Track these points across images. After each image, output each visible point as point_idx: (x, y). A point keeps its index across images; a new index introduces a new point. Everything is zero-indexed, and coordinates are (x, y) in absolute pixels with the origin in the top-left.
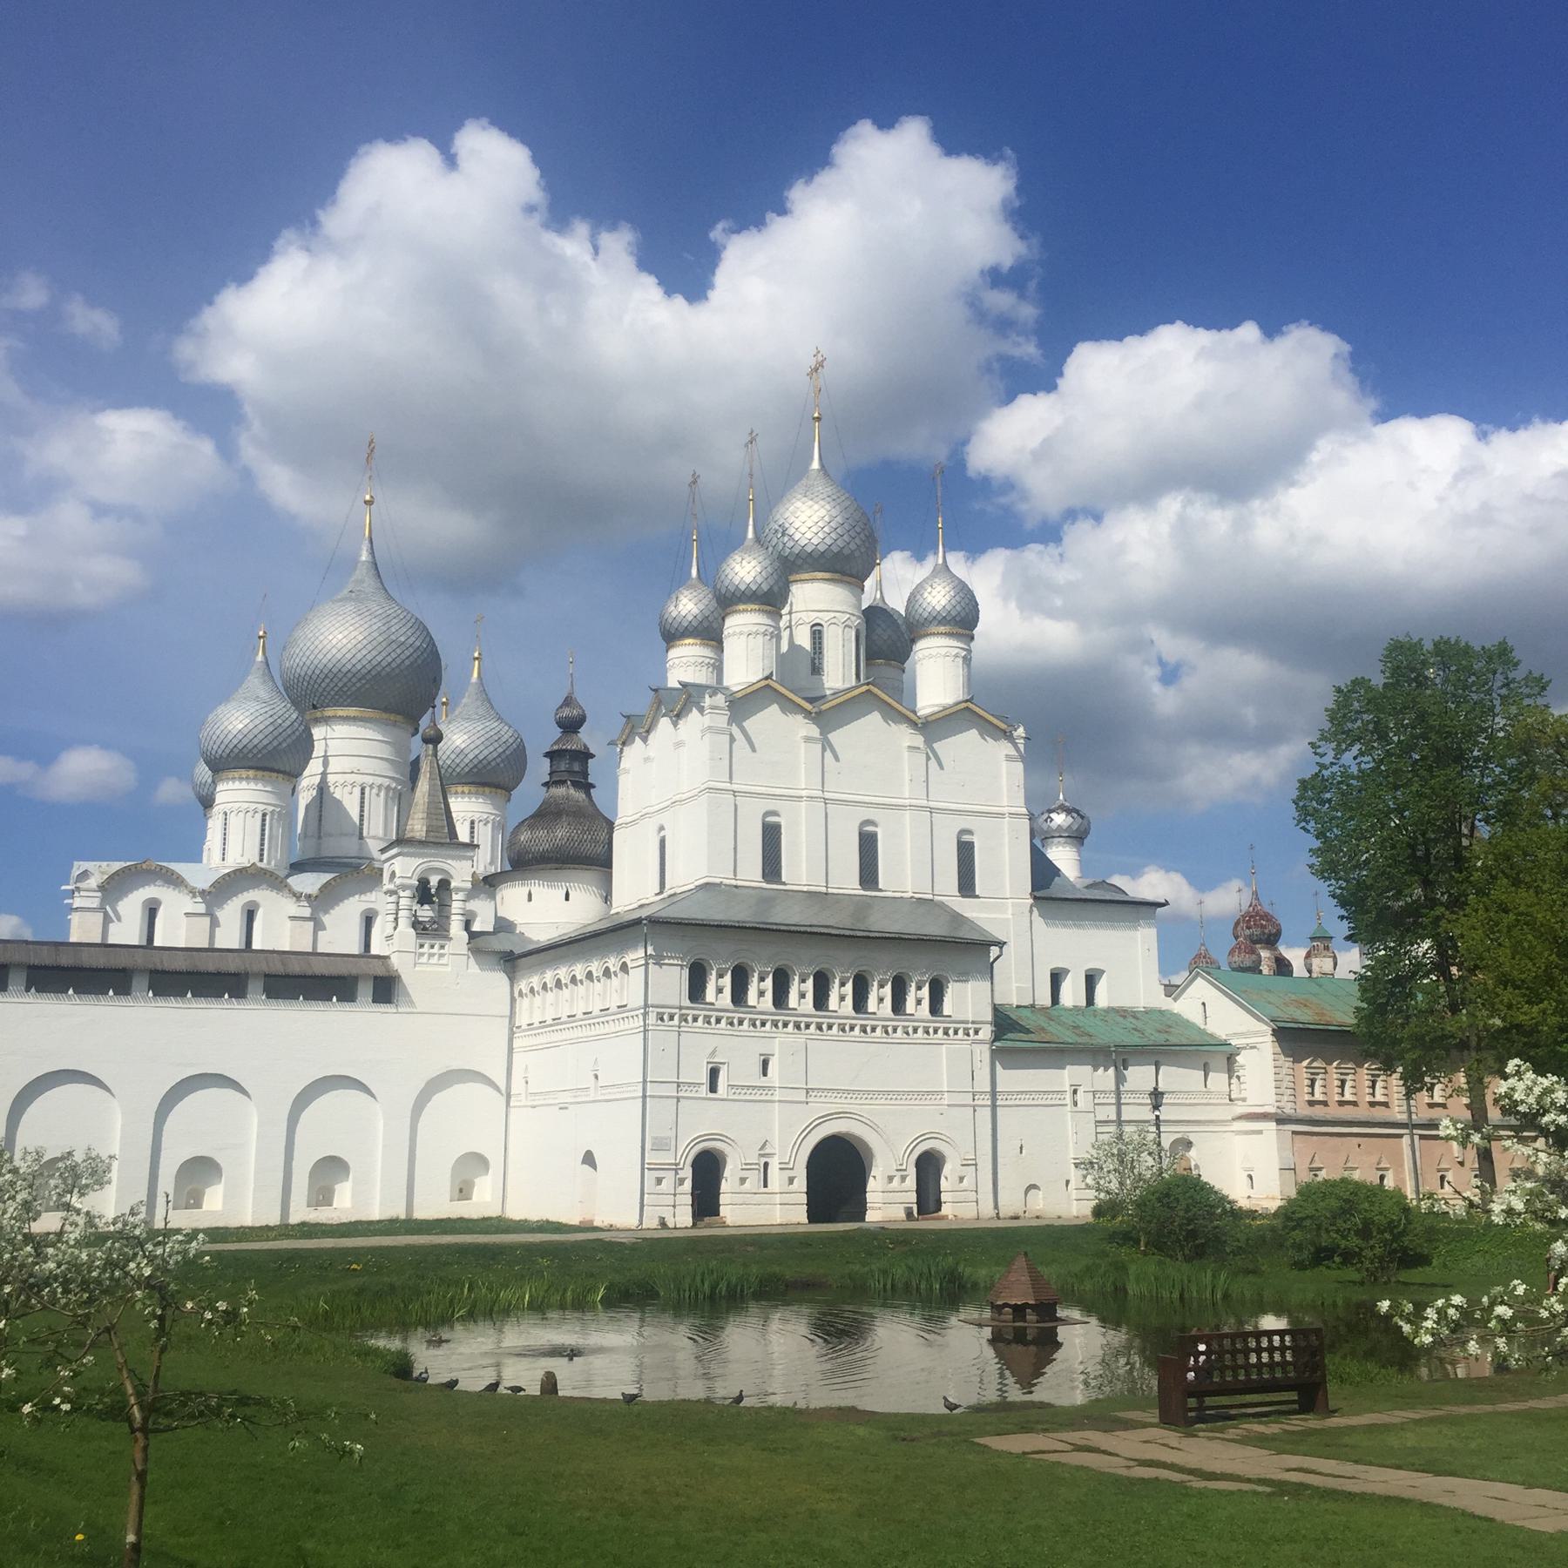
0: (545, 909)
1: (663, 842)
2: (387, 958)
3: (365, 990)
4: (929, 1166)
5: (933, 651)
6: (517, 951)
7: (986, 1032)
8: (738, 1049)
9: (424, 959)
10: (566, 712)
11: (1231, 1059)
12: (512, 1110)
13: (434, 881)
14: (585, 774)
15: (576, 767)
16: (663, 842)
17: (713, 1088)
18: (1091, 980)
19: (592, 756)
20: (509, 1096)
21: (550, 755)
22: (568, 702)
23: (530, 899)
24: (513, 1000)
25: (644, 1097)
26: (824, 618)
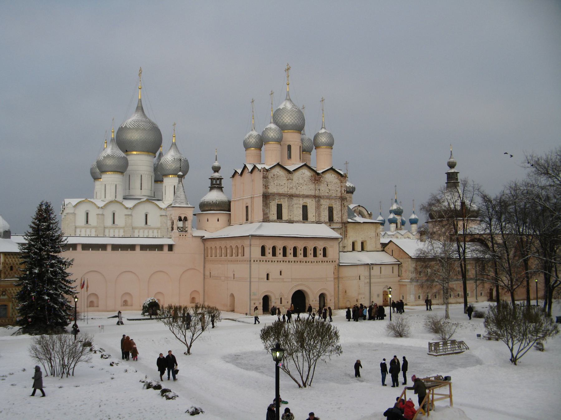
1: (247, 207)
3: (166, 249)
4: (322, 297)
8: (274, 268)
14: (220, 184)
15: (218, 182)
16: (247, 207)
17: (268, 279)
18: (362, 243)
25: (250, 282)
26: (291, 143)
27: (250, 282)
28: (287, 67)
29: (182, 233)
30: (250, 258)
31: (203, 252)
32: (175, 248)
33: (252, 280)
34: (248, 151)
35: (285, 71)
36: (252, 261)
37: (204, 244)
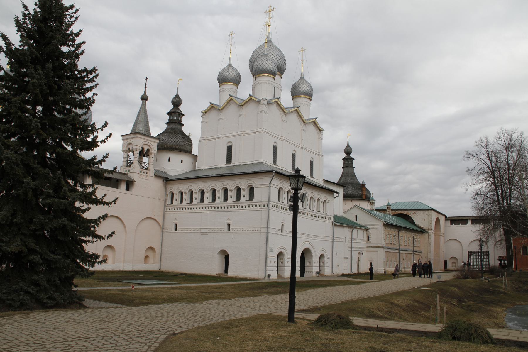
0: (176, 165)
2: (127, 174)
3: (123, 186)
5: (303, 103)
6: (170, 178)
7: (332, 220)
9: (141, 177)
10: (177, 100)
11: (367, 230)
12: (165, 234)
13: (145, 150)
19: (183, 115)
20: (163, 228)
21: (168, 114)
22: (177, 96)
23: (169, 161)
24: (166, 195)
27: (267, 233)
28: (268, 9)
29: (143, 171)
30: (269, 201)
31: (164, 198)
32: (135, 188)
33: (270, 231)
34: (223, 87)
35: (266, 12)
36: (270, 206)
37: (166, 187)
